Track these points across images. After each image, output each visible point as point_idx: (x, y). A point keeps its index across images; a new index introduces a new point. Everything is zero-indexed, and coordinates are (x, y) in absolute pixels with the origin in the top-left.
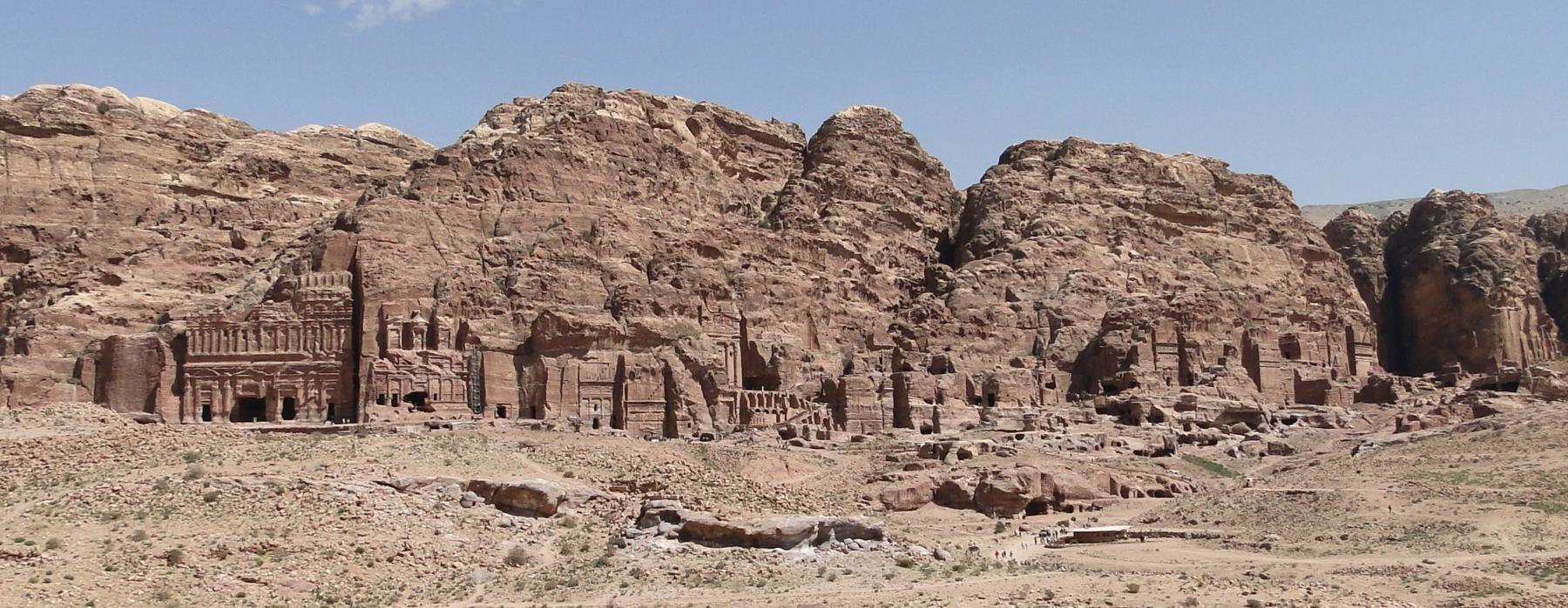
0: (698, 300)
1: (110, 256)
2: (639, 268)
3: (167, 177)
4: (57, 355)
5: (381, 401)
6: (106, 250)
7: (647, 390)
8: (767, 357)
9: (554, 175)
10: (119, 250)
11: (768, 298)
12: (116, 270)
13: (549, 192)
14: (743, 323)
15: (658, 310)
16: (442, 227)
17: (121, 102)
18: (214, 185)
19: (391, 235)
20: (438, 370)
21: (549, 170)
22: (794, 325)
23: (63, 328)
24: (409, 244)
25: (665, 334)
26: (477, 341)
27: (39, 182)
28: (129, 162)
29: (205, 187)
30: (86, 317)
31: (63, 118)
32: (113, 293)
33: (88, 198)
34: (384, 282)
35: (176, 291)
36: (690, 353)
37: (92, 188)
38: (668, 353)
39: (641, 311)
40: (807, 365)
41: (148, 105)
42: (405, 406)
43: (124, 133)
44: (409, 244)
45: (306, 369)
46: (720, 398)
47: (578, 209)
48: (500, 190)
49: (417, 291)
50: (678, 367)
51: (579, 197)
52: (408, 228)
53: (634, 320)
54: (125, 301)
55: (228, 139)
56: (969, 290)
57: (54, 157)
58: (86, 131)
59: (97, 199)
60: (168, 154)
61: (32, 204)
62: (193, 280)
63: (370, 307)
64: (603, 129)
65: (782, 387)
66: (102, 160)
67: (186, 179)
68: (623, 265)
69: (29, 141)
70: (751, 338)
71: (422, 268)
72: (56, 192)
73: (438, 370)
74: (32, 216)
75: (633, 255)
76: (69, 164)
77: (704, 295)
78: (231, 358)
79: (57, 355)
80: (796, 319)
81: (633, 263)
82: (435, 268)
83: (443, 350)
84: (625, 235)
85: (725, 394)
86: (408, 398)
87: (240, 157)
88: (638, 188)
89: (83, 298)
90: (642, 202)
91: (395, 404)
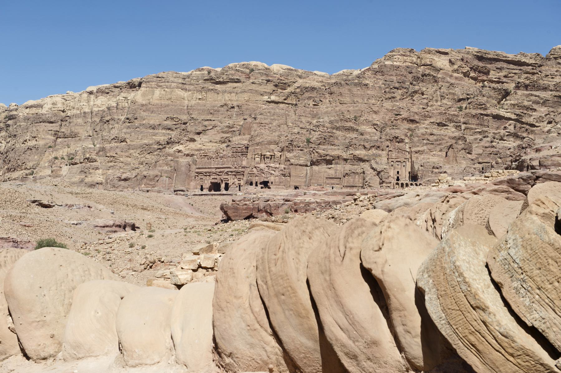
0: (388, 143)
1: (197, 131)
2: (377, 130)
3: (266, 98)
4: (166, 168)
5: (251, 184)
6: (196, 129)
7: (354, 181)
8: (416, 167)
10: (200, 129)
12: (196, 137)
13: (347, 99)
16: (294, 117)
17: (260, 67)
18: (285, 99)
19: (267, 121)
20: (273, 172)
21: (349, 90)
22: (440, 153)
23: (170, 158)
24: (274, 124)
25: (366, 158)
26: (289, 161)
27: (217, 102)
28: (251, 93)
29: (280, 101)
30: (180, 154)
31: (230, 77)
32: (192, 145)
33: (233, 107)
34: (258, 140)
35: (215, 144)
36: (374, 166)
37: (235, 104)
39: (356, 149)
40: (437, 170)
41: (276, 67)
42: (260, 186)
43: (251, 81)
44: (274, 124)
45: (231, 172)
46: (384, 184)
47: (357, 106)
48: (327, 100)
49: (270, 143)
51: (360, 101)
52: (276, 118)
53: (351, 153)
54: (196, 148)
55: (298, 79)
56: (555, 134)
57: (224, 92)
58: (238, 81)
59: (236, 108)
60: (270, 87)
61: (212, 111)
62: (223, 140)
64: (384, 70)
65: (419, 180)
66: (241, 92)
67: (273, 98)
68: (369, 129)
69: (218, 86)
70: (414, 159)
71: (277, 133)
72: (222, 106)
73: (273, 172)
74: (211, 116)
75: (374, 125)
76: (229, 95)
78: (209, 168)
79: (166, 168)
80: (441, 151)
81: (375, 128)
82: (283, 133)
84: (375, 116)
85: (387, 183)
86: (261, 183)
87: (298, 87)
88: (395, 95)
89: (181, 147)
90: (397, 101)
91: (256, 185)
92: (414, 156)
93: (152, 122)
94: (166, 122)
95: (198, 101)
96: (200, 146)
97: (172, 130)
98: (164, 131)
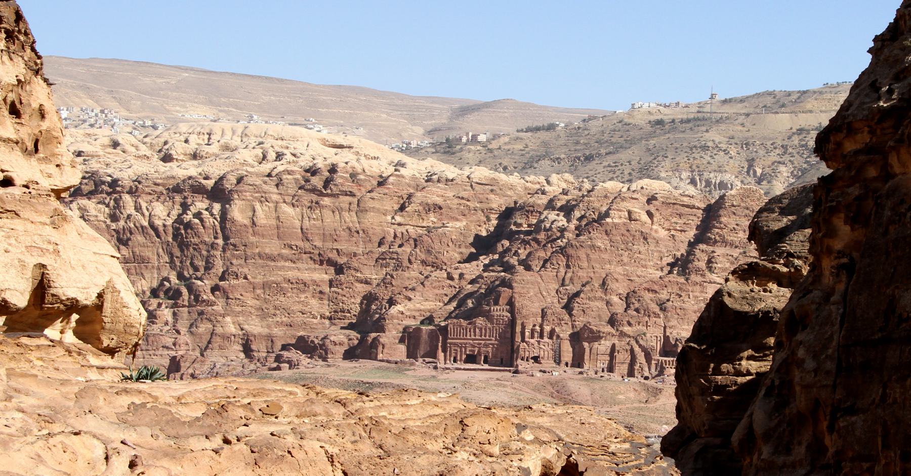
0: (647, 318)
5: (522, 359)
9: (588, 255)
11: (676, 316)
14: (665, 328)
15: (630, 324)
19: (525, 290)
25: (632, 334)
32: (410, 305)
36: (641, 342)
38: (633, 343)
50: (637, 349)
51: (598, 266)
59: (361, 232)
63: (519, 322)
68: (615, 299)
70: (668, 334)
77: (649, 316)
83: (546, 339)
90: (625, 264)
92: (668, 330)
93: (267, 251)
94: (283, 251)
95: (312, 222)
96: (418, 305)
97: (294, 262)
98: (287, 264)
